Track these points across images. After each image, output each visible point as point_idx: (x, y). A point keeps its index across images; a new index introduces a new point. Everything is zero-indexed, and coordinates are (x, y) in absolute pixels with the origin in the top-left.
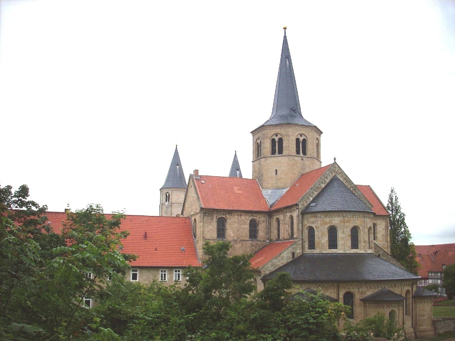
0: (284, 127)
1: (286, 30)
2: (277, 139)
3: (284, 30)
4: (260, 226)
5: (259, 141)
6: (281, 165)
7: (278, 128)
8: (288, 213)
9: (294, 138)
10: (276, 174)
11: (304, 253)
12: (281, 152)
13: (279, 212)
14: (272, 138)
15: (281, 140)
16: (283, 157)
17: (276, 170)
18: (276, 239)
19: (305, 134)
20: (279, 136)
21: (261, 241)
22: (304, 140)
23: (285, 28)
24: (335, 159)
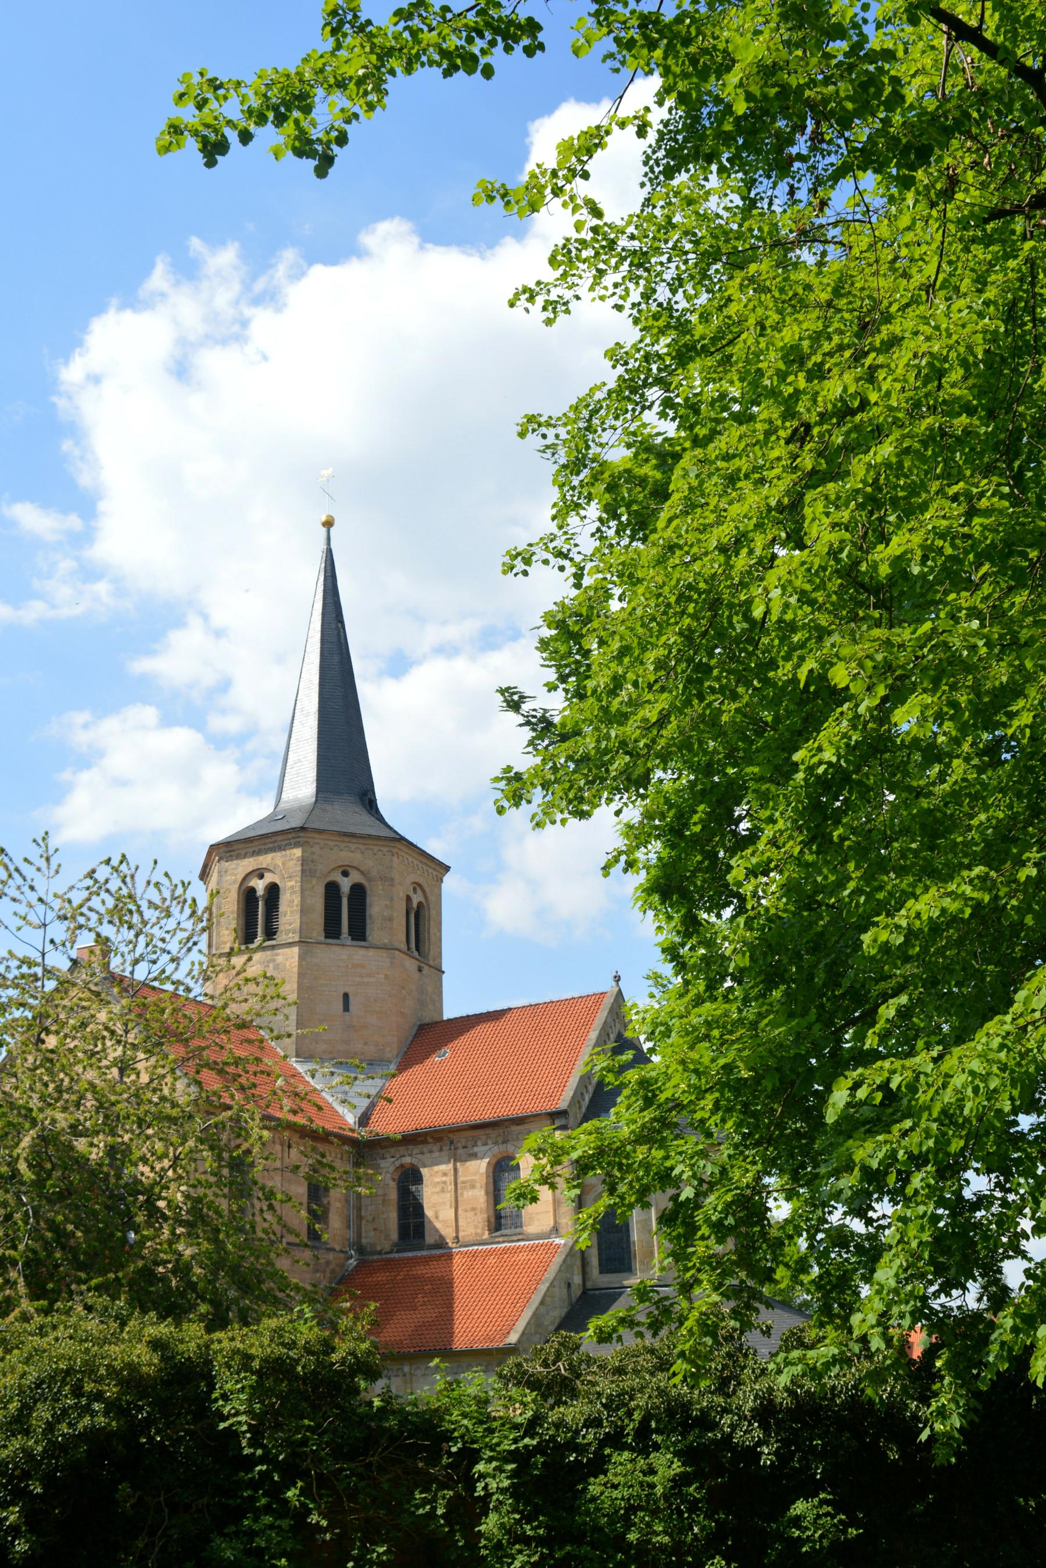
0: (376, 848)
1: (332, 530)
2: (345, 885)
3: (324, 530)
4: (332, 1192)
5: (260, 886)
6: (366, 980)
7: (353, 847)
8: (486, 1144)
9: (402, 895)
10: (346, 1008)
11: (589, 1285)
12: (359, 932)
13: (425, 1142)
14: (329, 879)
15: (359, 893)
16: (371, 952)
17: (346, 996)
18: (395, 1245)
19: (425, 886)
20: (355, 877)
21: (334, 1250)
22: (420, 904)
23: (328, 524)
24: (617, 979)
